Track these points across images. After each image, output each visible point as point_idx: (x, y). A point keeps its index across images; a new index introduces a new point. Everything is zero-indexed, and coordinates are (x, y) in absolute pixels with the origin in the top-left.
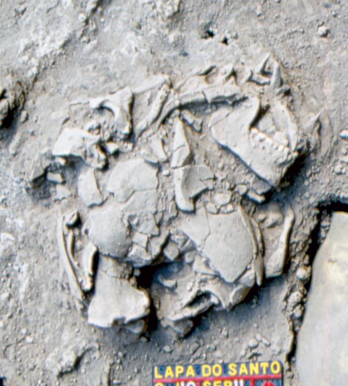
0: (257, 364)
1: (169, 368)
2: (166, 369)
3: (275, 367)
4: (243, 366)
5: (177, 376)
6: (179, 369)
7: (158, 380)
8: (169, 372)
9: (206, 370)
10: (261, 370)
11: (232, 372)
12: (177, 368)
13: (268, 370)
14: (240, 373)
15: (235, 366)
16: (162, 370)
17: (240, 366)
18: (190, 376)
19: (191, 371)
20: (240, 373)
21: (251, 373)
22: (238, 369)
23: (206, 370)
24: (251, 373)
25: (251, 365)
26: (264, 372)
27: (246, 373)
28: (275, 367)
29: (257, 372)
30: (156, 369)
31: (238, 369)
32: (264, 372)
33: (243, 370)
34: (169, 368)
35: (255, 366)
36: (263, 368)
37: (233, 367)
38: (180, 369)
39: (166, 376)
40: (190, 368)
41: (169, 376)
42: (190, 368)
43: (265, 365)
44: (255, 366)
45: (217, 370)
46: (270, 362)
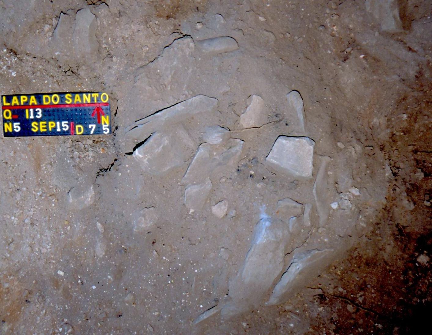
1: (15, 98)
2: (12, 98)
5: (22, 104)
9: (47, 99)
10: (92, 99)
12: (22, 97)
13: (99, 99)
14: (75, 102)
22: (73, 98)
23: (47, 99)
26: (95, 101)
27: (80, 102)
29: (89, 101)
30: (4, 98)
34: (15, 98)
35: (88, 96)
36: (94, 98)
38: (24, 99)
40: (33, 97)
44: (88, 96)
45: (55, 99)
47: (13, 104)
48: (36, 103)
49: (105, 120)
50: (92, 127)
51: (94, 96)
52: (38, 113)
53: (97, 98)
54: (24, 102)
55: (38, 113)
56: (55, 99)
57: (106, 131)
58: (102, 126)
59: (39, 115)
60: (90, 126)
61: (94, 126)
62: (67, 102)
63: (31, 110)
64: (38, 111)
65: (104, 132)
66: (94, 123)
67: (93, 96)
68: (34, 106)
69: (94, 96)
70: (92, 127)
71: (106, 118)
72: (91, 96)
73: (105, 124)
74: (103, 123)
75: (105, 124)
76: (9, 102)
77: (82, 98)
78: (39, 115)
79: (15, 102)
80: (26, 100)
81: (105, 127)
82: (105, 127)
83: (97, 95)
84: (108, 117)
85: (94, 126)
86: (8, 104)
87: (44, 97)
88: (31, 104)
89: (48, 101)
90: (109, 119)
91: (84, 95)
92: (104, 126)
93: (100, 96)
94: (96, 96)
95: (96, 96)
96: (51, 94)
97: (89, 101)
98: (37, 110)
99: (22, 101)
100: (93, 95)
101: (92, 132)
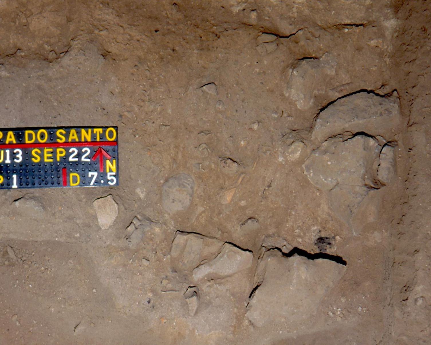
3: (111, 134)
9: (30, 136)
10: (94, 136)
13: (102, 136)
14: (70, 140)
22: (67, 136)
23: (30, 136)
24: (83, 140)
26: (98, 139)
27: (77, 140)
28: (111, 134)
29: (89, 139)
31: (67, 136)
32: (98, 139)
33: (73, 136)
35: (87, 132)
42: (10, 133)
44: (87, 132)
45: (42, 136)
48: (15, 142)
49: (110, 165)
50: (93, 176)
51: (97, 132)
52: (18, 156)
55: (18, 156)
56: (42, 136)
57: (112, 181)
58: (106, 174)
59: (18, 159)
60: (90, 174)
61: (96, 174)
62: (59, 141)
63: (8, 151)
64: (18, 153)
65: (110, 183)
66: (96, 171)
67: (95, 132)
68: (11, 146)
69: (97, 132)
70: (93, 176)
71: (112, 163)
72: (92, 132)
73: (111, 171)
74: (108, 170)
75: (111, 171)
77: (79, 134)
78: (18, 159)
81: (111, 176)
82: (111, 176)
83: (101, 130)
84: (114, 161)
85: (96, 174)
87: (27, 132)
88: (7, 142)
89: (32, 139)
90: (116, 163)
91: (83, 131)
92: (109, 174)
93: (104, 132)
94: (99, 132)
95: (99, 132)
97: (89, 139)
98: (15, 151)
100: (95, 130)
101: (92, 183)
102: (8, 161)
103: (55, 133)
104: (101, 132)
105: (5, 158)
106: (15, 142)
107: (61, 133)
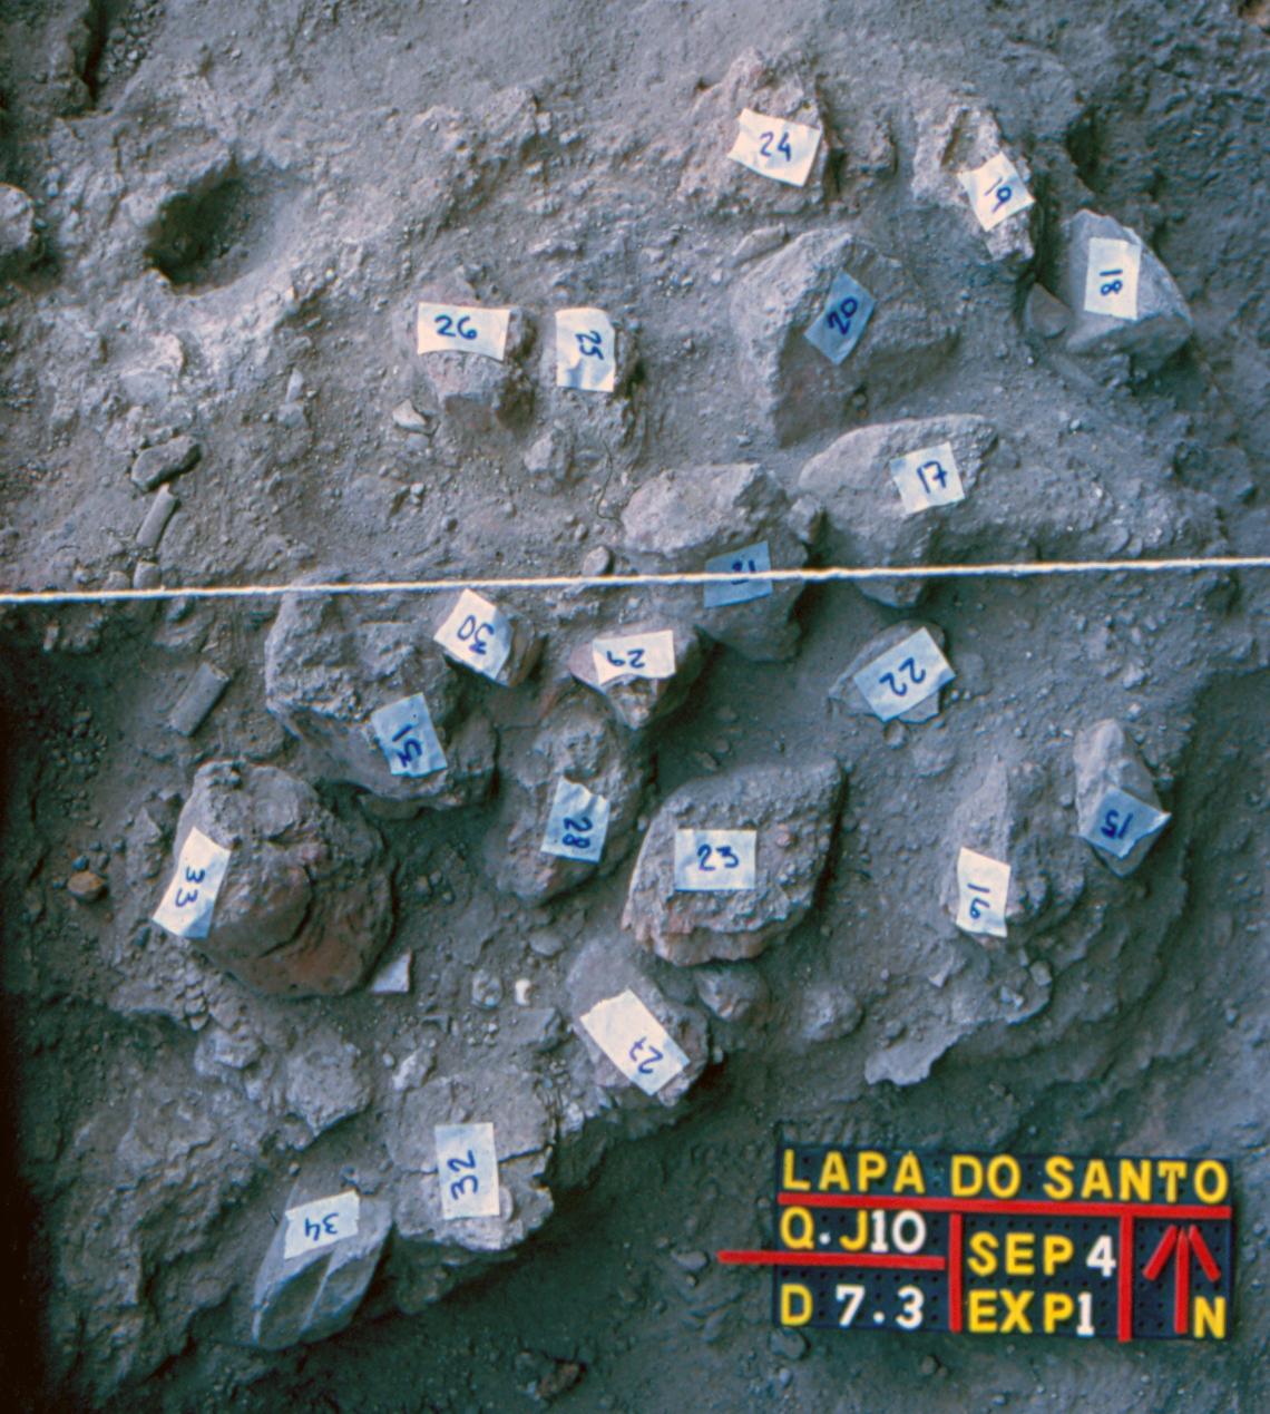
0: (1146, 1166)
1: (834, 1158)
2: (823, 1160)
4: (1096, 1166)
5: (863, 1186)
6: (871, 1165)
7: (796, 1198)
8: (833, 1172)
9: (967, 1175)
10: (1158, 1185)
11: (1058, 1186)
12: (864, 1158)
13: (1185, 1186)
14: (1086, 1193)
15: (1068, 1166)
16: (809, 1166)
17: (1085, 1169)
18: (909, 1189)
19: (910, 1174)
20: (1086, 1193)
21: (1125, 1195)
22: (1077, 1177)
23: (967, 1175)
24: (1125, 1195)
25: (1126, 1169)
26: (1171, 1195)
29: (1144, 1193)
30: (789, 1156)
31: (1077, 1177)
32: (1171, 1195)
33: (1096, 1178)
34: (834, 1158)
36: (1165, 1180)
37: (1059, 1169)
38: (872, 1165)
39: (823, 1185)
40: (909, 1161)
41: (834, 1187)
42: (909, 1161)
43: (1173, 1170)
45: (1003, 1176)
46: (1192, 1164)
47: (823, 1185)
48: (920, 1188)
53: (1179, 1182)
54: (871, 1181)
56: (1003, 1176)
62: (1049, 1189)
67: (1162, 1173)
72: (1154, 1170)
76: (806, 1178)
79: (834, 1179)
80: (879, 1172)
86: (804, 1186)
88: (898, 1187)
96: (985, 1157)
99: (864, 1175)
100: (1163, 1167)
102: (879, 1246)
103: (1042, 1168)
104: (1182, 1174)
105: (871, 1237)
106: (920, 1188)
107: (1059, 1169)
